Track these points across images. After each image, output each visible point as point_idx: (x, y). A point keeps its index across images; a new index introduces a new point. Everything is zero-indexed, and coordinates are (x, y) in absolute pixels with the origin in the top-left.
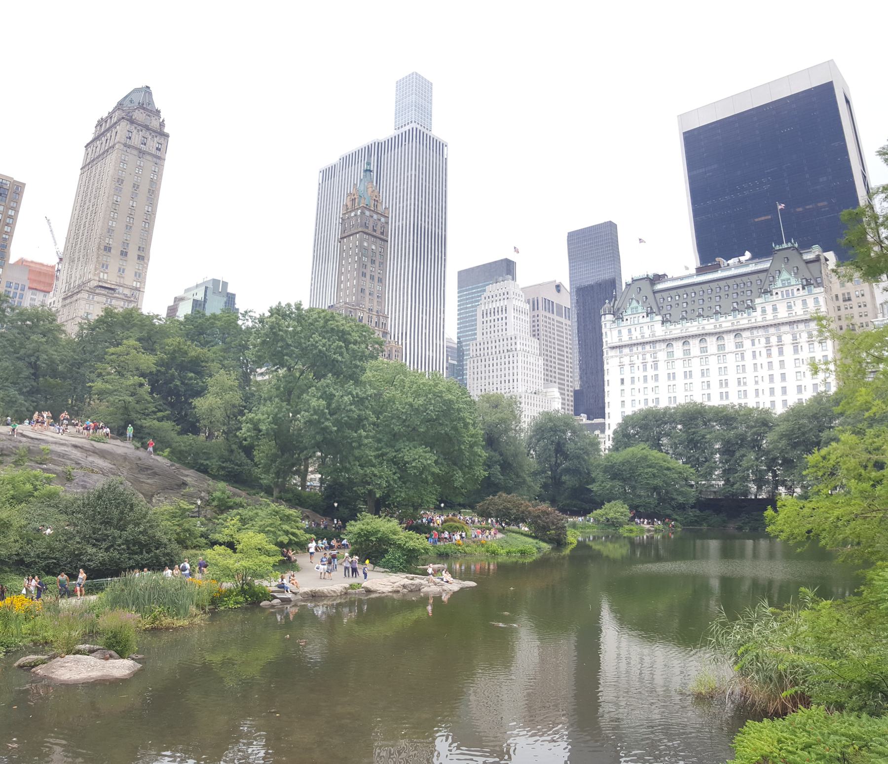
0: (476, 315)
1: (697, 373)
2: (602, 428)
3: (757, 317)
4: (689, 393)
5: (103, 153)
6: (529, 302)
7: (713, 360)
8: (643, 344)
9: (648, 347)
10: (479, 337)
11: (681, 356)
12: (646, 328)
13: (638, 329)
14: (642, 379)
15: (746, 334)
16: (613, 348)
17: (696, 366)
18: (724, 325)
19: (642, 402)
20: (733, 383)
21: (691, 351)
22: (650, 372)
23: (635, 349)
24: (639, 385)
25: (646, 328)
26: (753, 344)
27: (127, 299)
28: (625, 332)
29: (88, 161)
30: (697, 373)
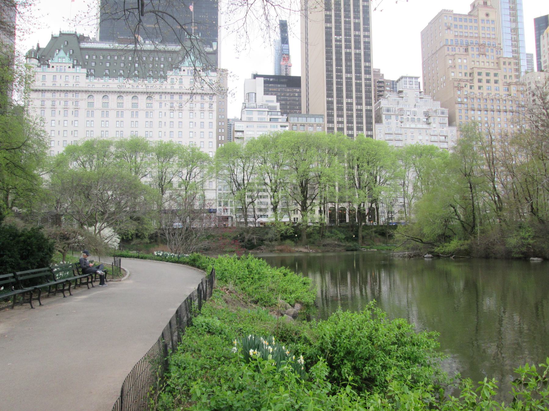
3: (166, 86)
8: (67, 91)
9: (70, 95)
12: (71, 77)
13: (63, 77)
22: (71, 118)
25: (71, 77)
26: (160, 106)
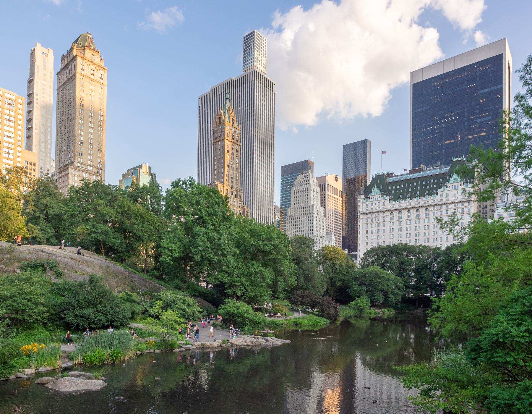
0: (291, 193)
1: (404, 229)
2: (356, 257)
4: (400, 239)
5: (69, 79)
6: (319, 186)
7: (413, 222)
8: (378, 212)
9: (381, 214)
10: (293, 206)
11: (406, 218)
12: (381, 203)
13: (377, 203)
14: (377, 231)
15: (431, 208)
16: (363, 214)
17: (404, 225)
18: (421, 203)
19: (376, 243)
20: (422, 234)
21: (403, 217)
22: (381, 228)
23: (374, 214)
24: (375, 234)
25: (381, 203)
27: (97, 174)
28: (370, 205)
29: (61, 84)
30: (404, 229)
